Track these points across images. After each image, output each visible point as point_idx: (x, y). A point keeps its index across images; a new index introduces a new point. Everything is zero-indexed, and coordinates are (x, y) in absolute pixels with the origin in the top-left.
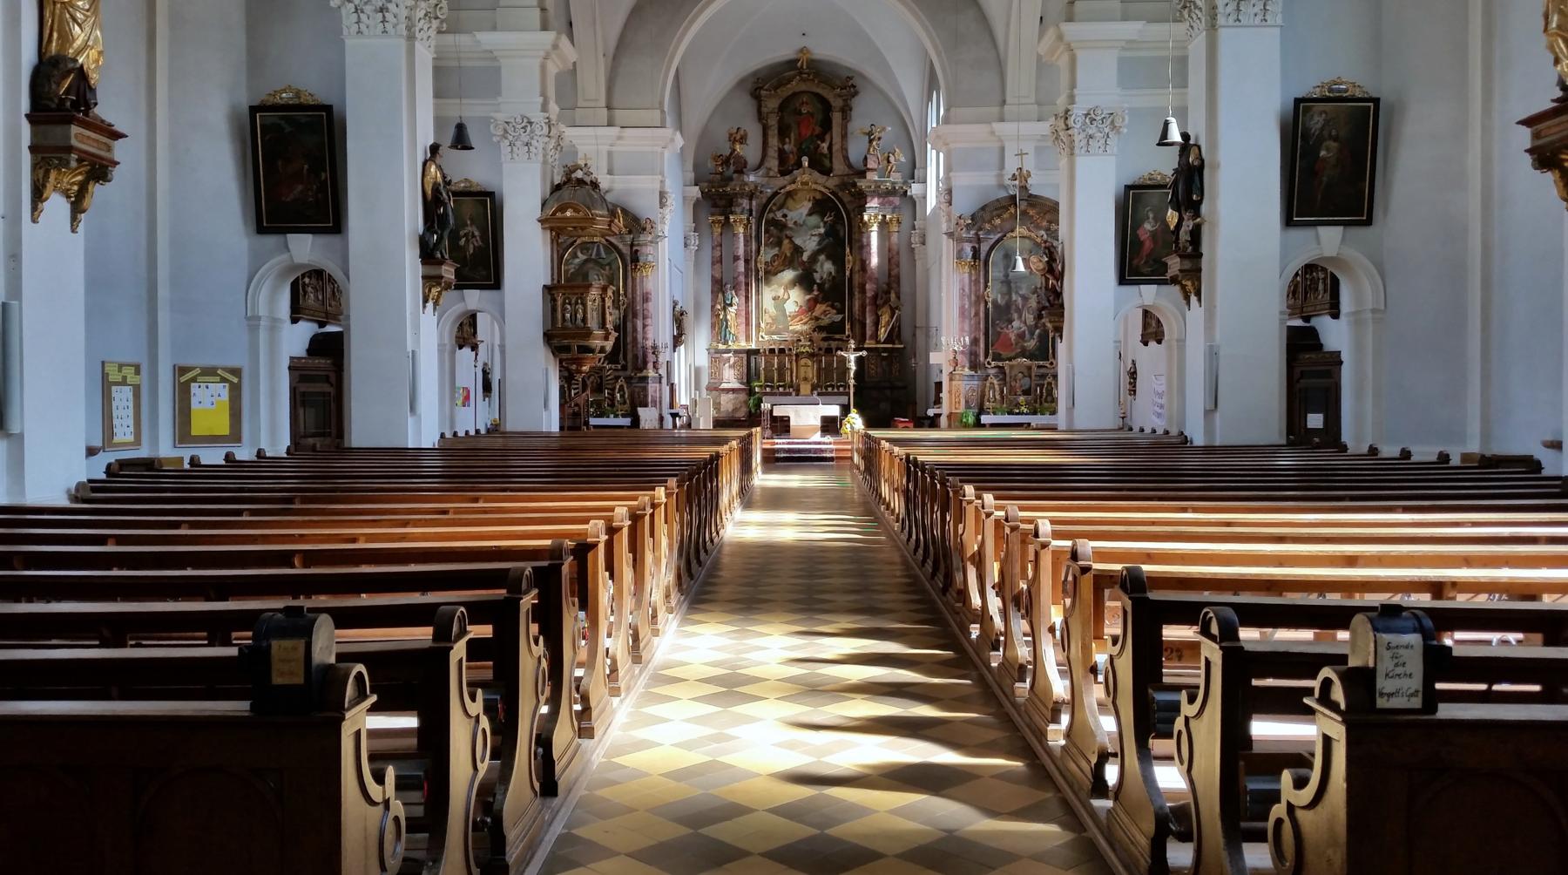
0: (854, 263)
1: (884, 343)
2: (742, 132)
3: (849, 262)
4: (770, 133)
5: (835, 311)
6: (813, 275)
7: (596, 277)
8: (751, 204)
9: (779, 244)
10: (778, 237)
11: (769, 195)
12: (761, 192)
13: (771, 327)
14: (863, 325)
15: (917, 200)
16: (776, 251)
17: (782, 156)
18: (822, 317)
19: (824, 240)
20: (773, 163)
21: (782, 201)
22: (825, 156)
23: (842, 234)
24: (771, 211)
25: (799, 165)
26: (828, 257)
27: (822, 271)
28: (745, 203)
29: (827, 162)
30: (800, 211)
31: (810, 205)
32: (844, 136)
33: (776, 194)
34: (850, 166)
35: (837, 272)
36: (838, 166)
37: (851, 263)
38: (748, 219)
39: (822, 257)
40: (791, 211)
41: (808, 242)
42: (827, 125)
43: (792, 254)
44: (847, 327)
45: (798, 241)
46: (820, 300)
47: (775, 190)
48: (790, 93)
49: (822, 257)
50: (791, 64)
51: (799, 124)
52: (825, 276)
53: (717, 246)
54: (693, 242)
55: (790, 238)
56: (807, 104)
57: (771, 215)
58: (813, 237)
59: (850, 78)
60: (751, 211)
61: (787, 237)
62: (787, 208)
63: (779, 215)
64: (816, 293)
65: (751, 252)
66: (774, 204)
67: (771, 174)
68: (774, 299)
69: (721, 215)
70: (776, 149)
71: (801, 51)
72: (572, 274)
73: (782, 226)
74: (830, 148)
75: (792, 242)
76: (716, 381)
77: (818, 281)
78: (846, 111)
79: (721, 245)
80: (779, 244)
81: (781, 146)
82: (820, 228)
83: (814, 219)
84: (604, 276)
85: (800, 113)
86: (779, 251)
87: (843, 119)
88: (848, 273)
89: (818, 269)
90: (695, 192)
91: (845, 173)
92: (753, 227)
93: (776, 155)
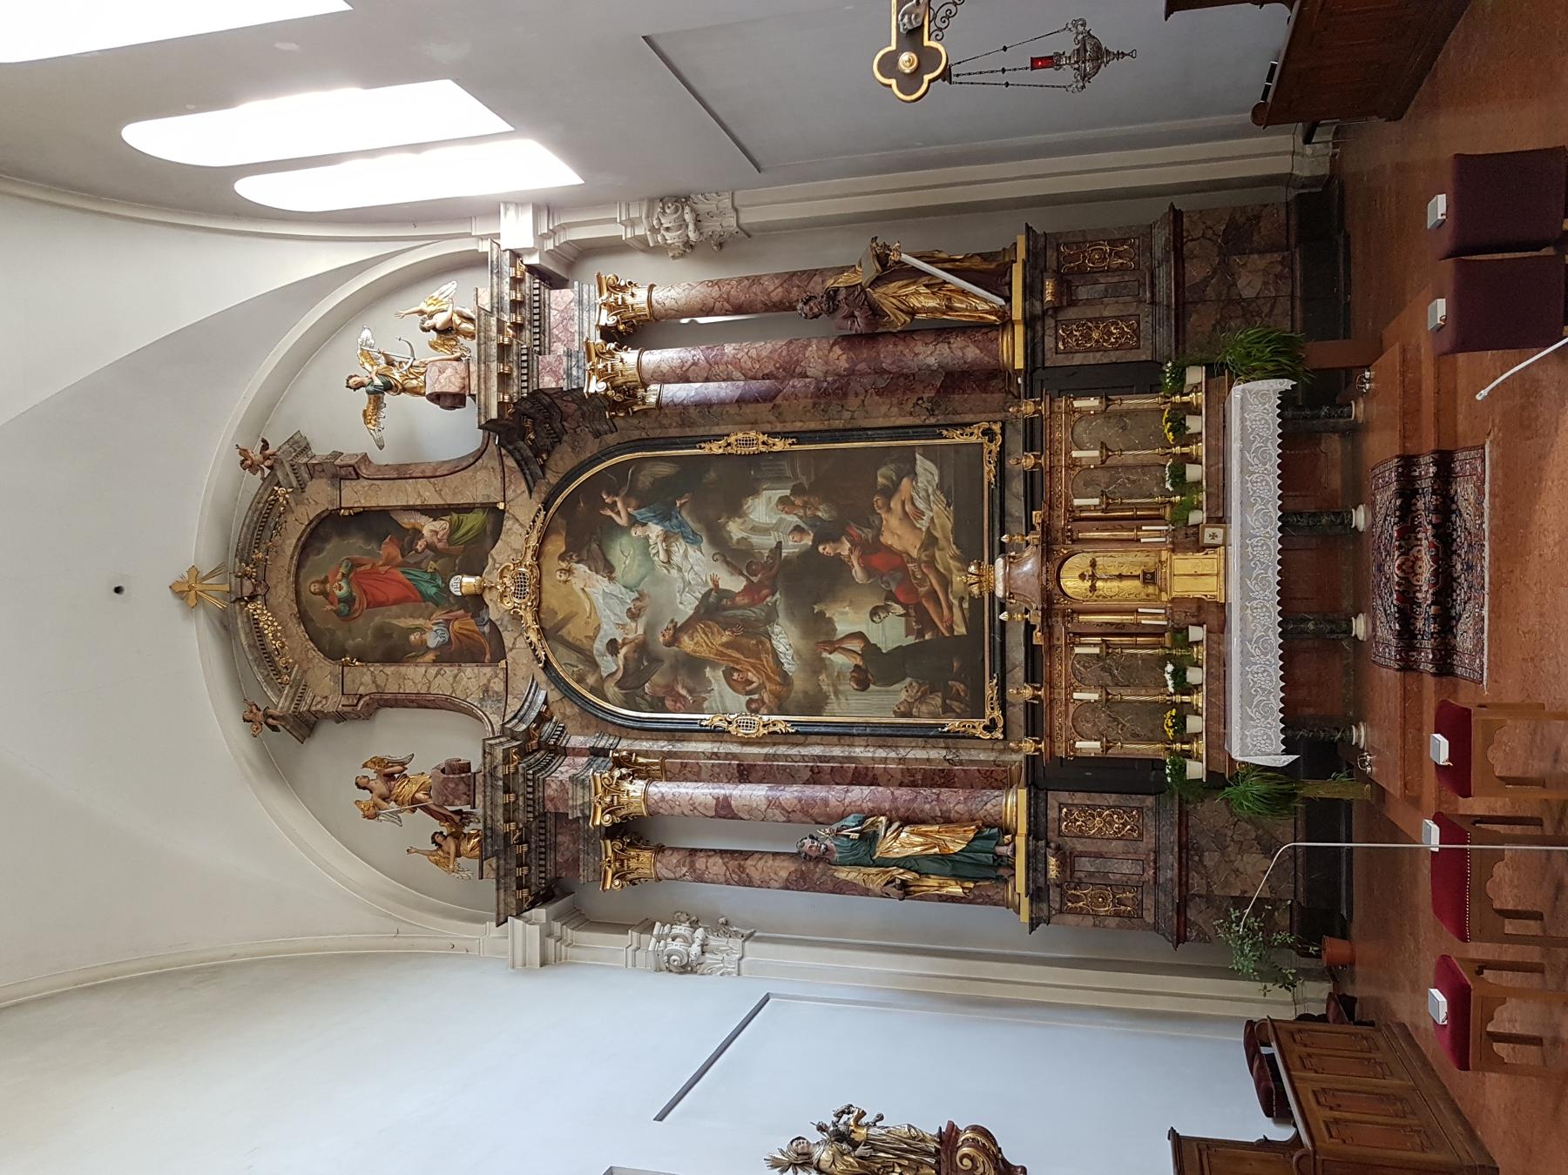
0: (754, 424)
1: (1008, 299)
2: (371, 773)
3: (748, 442)
4: (392, 688)
5: (905, 481)
6: (788, 560)
8: (577, 752)
9: (693, 666)
10: (675, 668)
11: (555, 696)
12: (542, 719)
13: (957, 697)
14: (955, 380)
15: (564, 237)
16: (715, 677)
17: (457, 653)
18: (923, 524)
19: (682, 525)
20: (470, 679)
21: (573, 657)
22: (454, 529)
23: (665, 470)
24: (598, 691)
25: (475, 603)
26: (736, 510)
27: (776, 527)
28: (564, 771)
29: (473, 521)
30: (599, 601)
31: (581, 568)
32: (401, 473)
33: (547, 666)
34: (479, 454)
35: (779, 479)
36: (481, 487)
37: (753, 434)
38: (618, 763)
39: (735, 529)
40: (598, 628)
41: (689, 576)
42: (374, 522)
43: (726, 625)
44: (958, 438)
45: (687, 606)
46: (868, 534)
47: (542, 677)
48: (298, 630)
49: (735, 529)
50: (226, 627)
51: (375, 604)
52: (793, 519)
53: (692, 866)
54: (677, 945)
55: (677, 631)
56: (325, 581)
57: (611, 689)
58: (676, 559)
59: (243, 452)
60: (596, 753)
61: (674, 641)
62: (593, 639)
63: (610, 665)
64: (845, 548)
65: (716, 755)
66: (580, 680)
67: (497, 686)
68: (863, 685)
69: (598, 852)
70: (433, 670)
71: (181, 592)
73: (643, 655)
74: (434, 512)
75: (689, 626)
76: (1149, 902)
77: (808, 541)
78: (344, 471)
79: (693, 852)
80: (693, 666)
81: (430, 657)
82: (647, 538)
83: (623, 553)
85: (349, 600)
86: (714, 665)
87: (358, 476)
88: (780, 445)
89: (770, 541)
90: (526, 931)
91: (496, 464)
92: (645, 745)
93: (449, 671)
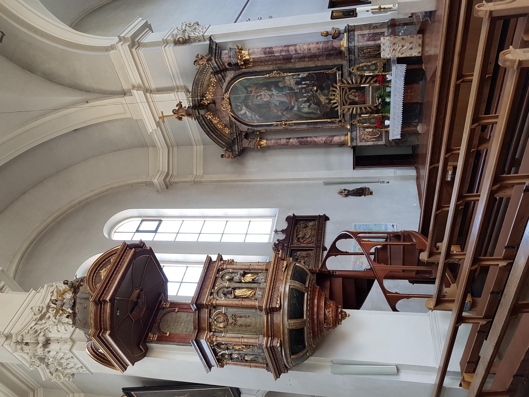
7: (259, 98)
72: (260, 117)
84: (257, 91)
